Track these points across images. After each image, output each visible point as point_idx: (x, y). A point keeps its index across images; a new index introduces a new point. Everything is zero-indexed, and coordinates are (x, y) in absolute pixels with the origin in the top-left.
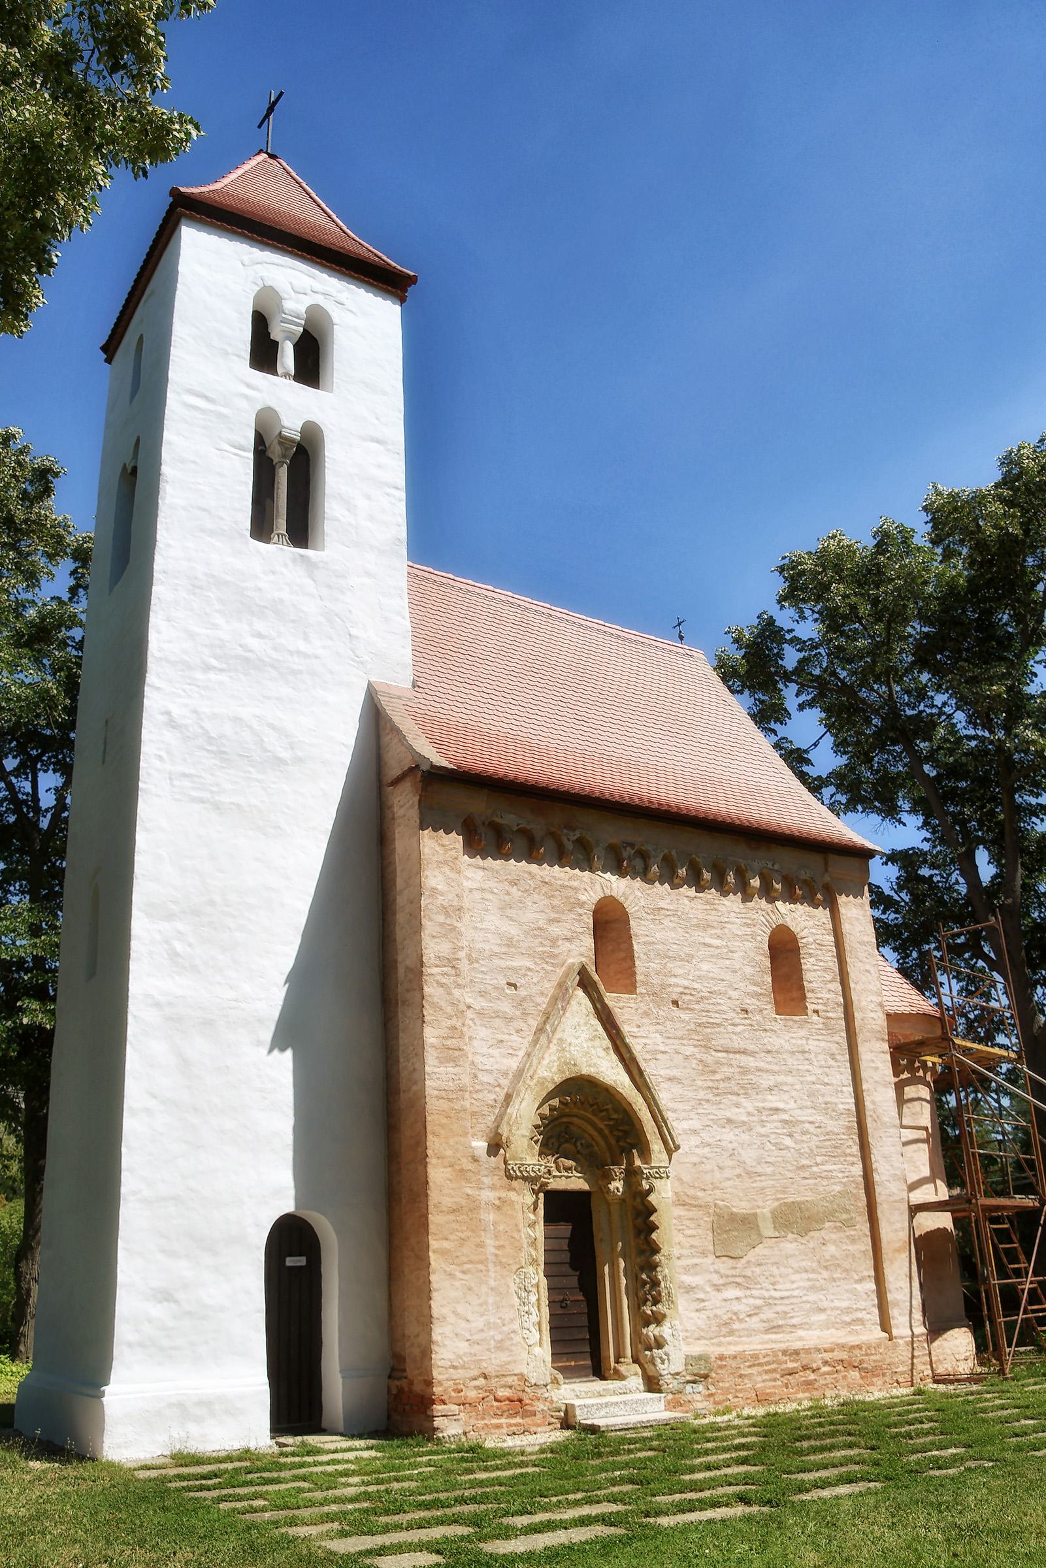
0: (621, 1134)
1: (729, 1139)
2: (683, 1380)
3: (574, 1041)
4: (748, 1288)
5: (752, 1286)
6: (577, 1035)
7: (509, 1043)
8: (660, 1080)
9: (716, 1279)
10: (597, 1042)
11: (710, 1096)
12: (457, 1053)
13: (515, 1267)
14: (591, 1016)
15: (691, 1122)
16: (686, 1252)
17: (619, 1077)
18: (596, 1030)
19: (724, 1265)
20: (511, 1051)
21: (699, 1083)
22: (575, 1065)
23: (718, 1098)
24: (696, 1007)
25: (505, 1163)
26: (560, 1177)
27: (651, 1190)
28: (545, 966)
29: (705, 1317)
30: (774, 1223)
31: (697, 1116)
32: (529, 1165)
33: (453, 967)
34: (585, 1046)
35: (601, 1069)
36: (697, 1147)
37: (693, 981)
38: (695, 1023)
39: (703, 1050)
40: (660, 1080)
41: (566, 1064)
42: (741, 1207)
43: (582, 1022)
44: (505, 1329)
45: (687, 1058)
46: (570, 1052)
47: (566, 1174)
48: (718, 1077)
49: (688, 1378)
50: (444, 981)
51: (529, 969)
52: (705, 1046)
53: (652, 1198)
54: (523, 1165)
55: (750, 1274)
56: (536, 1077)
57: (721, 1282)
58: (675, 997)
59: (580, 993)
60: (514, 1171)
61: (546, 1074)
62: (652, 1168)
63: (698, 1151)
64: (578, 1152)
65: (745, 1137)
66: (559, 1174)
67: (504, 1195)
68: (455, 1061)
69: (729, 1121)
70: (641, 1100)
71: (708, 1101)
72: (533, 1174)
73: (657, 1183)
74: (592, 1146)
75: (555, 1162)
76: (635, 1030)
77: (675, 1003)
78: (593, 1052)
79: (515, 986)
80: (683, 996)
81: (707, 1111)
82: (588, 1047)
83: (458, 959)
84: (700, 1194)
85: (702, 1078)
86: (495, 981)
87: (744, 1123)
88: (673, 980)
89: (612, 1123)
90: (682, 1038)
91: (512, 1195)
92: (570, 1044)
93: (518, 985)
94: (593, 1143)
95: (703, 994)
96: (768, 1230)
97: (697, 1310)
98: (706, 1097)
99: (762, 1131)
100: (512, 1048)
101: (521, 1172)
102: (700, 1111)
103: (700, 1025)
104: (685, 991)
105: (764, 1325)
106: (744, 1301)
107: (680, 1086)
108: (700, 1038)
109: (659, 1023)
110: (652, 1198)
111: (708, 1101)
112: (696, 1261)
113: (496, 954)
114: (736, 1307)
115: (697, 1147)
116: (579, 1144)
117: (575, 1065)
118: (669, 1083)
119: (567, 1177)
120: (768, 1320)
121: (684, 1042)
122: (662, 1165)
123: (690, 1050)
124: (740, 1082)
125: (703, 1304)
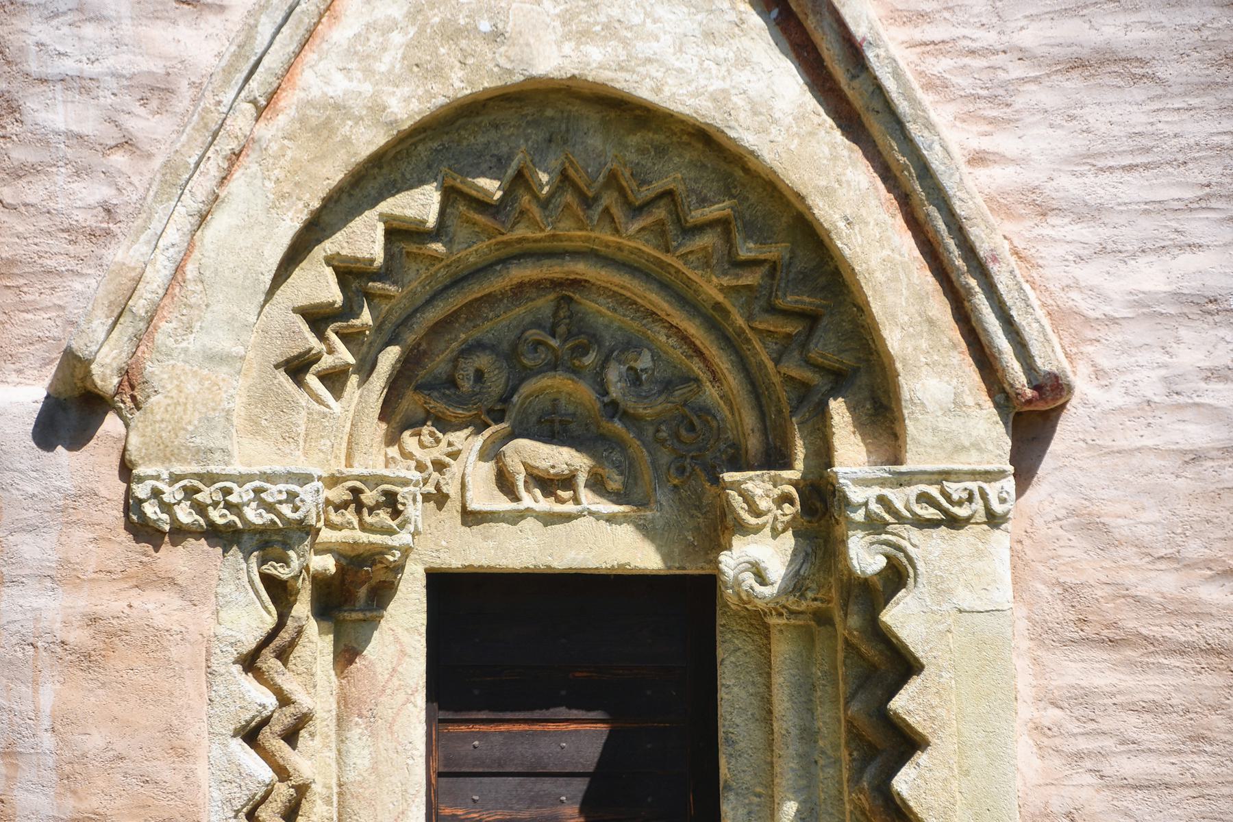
0: (791, 328)
22: (497, 36)
25: (126, 470)
26: (515, 518)
32: (242, 479)
35: (643, 48)
47: (545, 504)
54: (210, 479)
56: (289, 101)
60: (166, 507)
61: (339, 86)
64: (613, 409)
66: (503, 504)
67: (118, 606)
72: (254, 515)
74: (689, 379)
75: (491, 453)
89: (750, 278)
94: (696, 367)
101: (201, 509)
116: (614, 374)
117: (497, 36)
119: (549, 519)
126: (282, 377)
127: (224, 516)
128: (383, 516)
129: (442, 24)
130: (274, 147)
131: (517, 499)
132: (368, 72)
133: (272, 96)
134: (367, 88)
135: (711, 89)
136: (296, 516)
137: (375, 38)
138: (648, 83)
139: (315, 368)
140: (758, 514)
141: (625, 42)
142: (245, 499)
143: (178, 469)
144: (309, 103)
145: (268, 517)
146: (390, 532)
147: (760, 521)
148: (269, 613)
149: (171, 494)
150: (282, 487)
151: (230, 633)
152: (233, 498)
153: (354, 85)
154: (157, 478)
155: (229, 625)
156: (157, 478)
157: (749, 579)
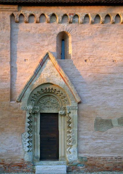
1: (103, 99)
4: (105, 140)
5: (107, 139)
9: (94, 137)
11: (97, 87)
12: (6, 79)
19: (96, 134)
23: (100, 87)
30: (119, 122)
31: (91, 93)
42: (105, 118)
48: (101, 81)
55: (107, 136)
57: (95, 138)
63: (91, 102)
65: (110, 98)
69: (103, 93)
81: (96, 91)
82: (50, 75)
87: (110, 94)
96: (115, 124)
98: (96, 87)
99: (117, 96)
105: (111, 150)
106: (104, 143)
111: (96, 88)
114: (100, 144)
115: (90, 101)
118: (82, 83)
120: (112, 149)
122: (75, 106)
124: (110, 82)
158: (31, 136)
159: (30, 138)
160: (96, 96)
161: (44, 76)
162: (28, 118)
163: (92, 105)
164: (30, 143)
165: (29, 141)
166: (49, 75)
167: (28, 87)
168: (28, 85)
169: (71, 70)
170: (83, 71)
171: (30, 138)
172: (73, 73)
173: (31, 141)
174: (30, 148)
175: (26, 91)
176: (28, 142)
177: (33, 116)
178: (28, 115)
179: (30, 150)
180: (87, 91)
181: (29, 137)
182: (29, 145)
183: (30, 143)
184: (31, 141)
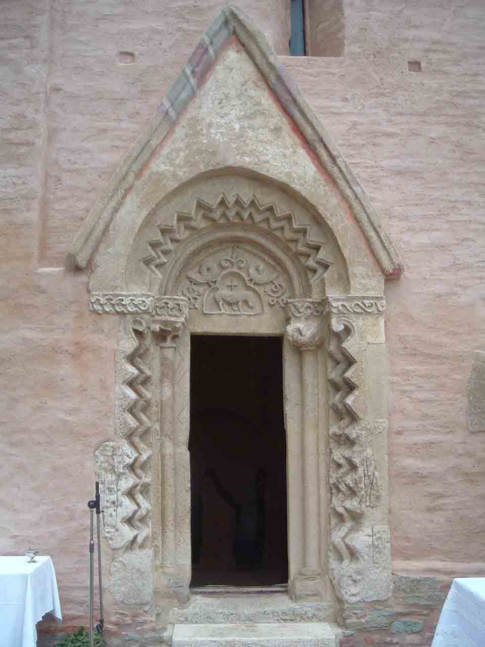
2: (388, 611)
3: (217, 120)
6: (223, 112)
7: (117, 133)
8: (381, 173)
10: (258, 121)
12: (22, 150)
13: (95, 441)
14: (250, 84)
15: (435, 234)
16: (412, 424)
17: (295, 168)
18: (259, 104)
20: (117, 143)
21: (456, 178)
24: (454, 69)
27: (348, 331)
28: (185, 26)
29: (442, 520)
31: (446, 226)
33: (27, 37)
34: (237, 126)
36: (444, 269)
37: (449, 33)
38: (450, 93)
39: (465, 129)
40: (381, 173)
41: (200, 152)
43: (233, 93)
44: (74, 524)
45: (432, 141)
46: (208, 135)
49: (399, 609)
50: (12, 56)
51: (157, 32)
52: (468, 125)
53: (351, 345)
56: (146, 173)
58: (413, 56)
59: (233, 56)
62: (350, 299)
68: (19, 161)
70: (334, 200)
71: (469, 203)
73: (358, 323)
76: (340, 104)
77: (415, 65)
78: (250, 133)
79: (131, 55)
80: (431, 55)
82: (242, 128)
83: (35, 26)
84: (445, 340)
85: (461, 170)
86: (100, 52)
88: (412, 33)
90: (424, 114)
91: (96, 339)
92: (210, 125)
93: (136, 53)
95: (467, 50)
97: (429, 510)
100: (119, 138)
102: (453, 217)
103: (459, 94)
104: (434, 47)
107: (417, 182)
108: (460, 112)
109: (382, 95)
110: (351, 345)
111: (469, 203)
112: (429, 437)
113: (105, 17)
115: (444, 269)
121: (427, 119)
122: (372, 294)
123: (437, 131)
125: (441, 501)
126: (142, 264)
127: (120, 308)
128: (175, 312)
129: (197, 149)
130: (140, 187)
131: (220, 310)
132: (172, 165)
133: (141, 170)
134: (172, 169)
135: (285, 171)
136: (145, 309)
137: (174, 154)
138: (265, 169)
139: (153, 263)
140: (300, 313)
141: (257, 156)
142: (128, 303)
143: (105, 293)
144: (152, 173)
145: (135, 309)
146: (178, 317)
147: (301, 315)
148: (136, 342)
149: (103, 301)
150: (140, 299)
151: (122, 348)
152: (123, 303)
153: (167, 168)
154: (98, 295)
155: (121, 346)
156: (98, 295)
157: (296, 335)
158: (144, 457)
159: (139, 471)
160: (470, 243)
161: (212, 131)
162: (131, 359)
163: (454, 294)
164: (140, 498)
165: (135, 486)
166: (237, 126)
167: (128, 190)
168: (130, 179)
169: (344, 110)
170: (401, 114)
171: (139, 471)
172: (355, 124)
173: (145, 489)
174: (138, 528)
175: (122, 212)
176: (130, 494)
177: (154, 350)
178: (129, 344)
179: (140, 540)
180: (424, 217)
181: (132, 467)
182: (135, 512)
183: (140, 498)
184: (145, 489)
